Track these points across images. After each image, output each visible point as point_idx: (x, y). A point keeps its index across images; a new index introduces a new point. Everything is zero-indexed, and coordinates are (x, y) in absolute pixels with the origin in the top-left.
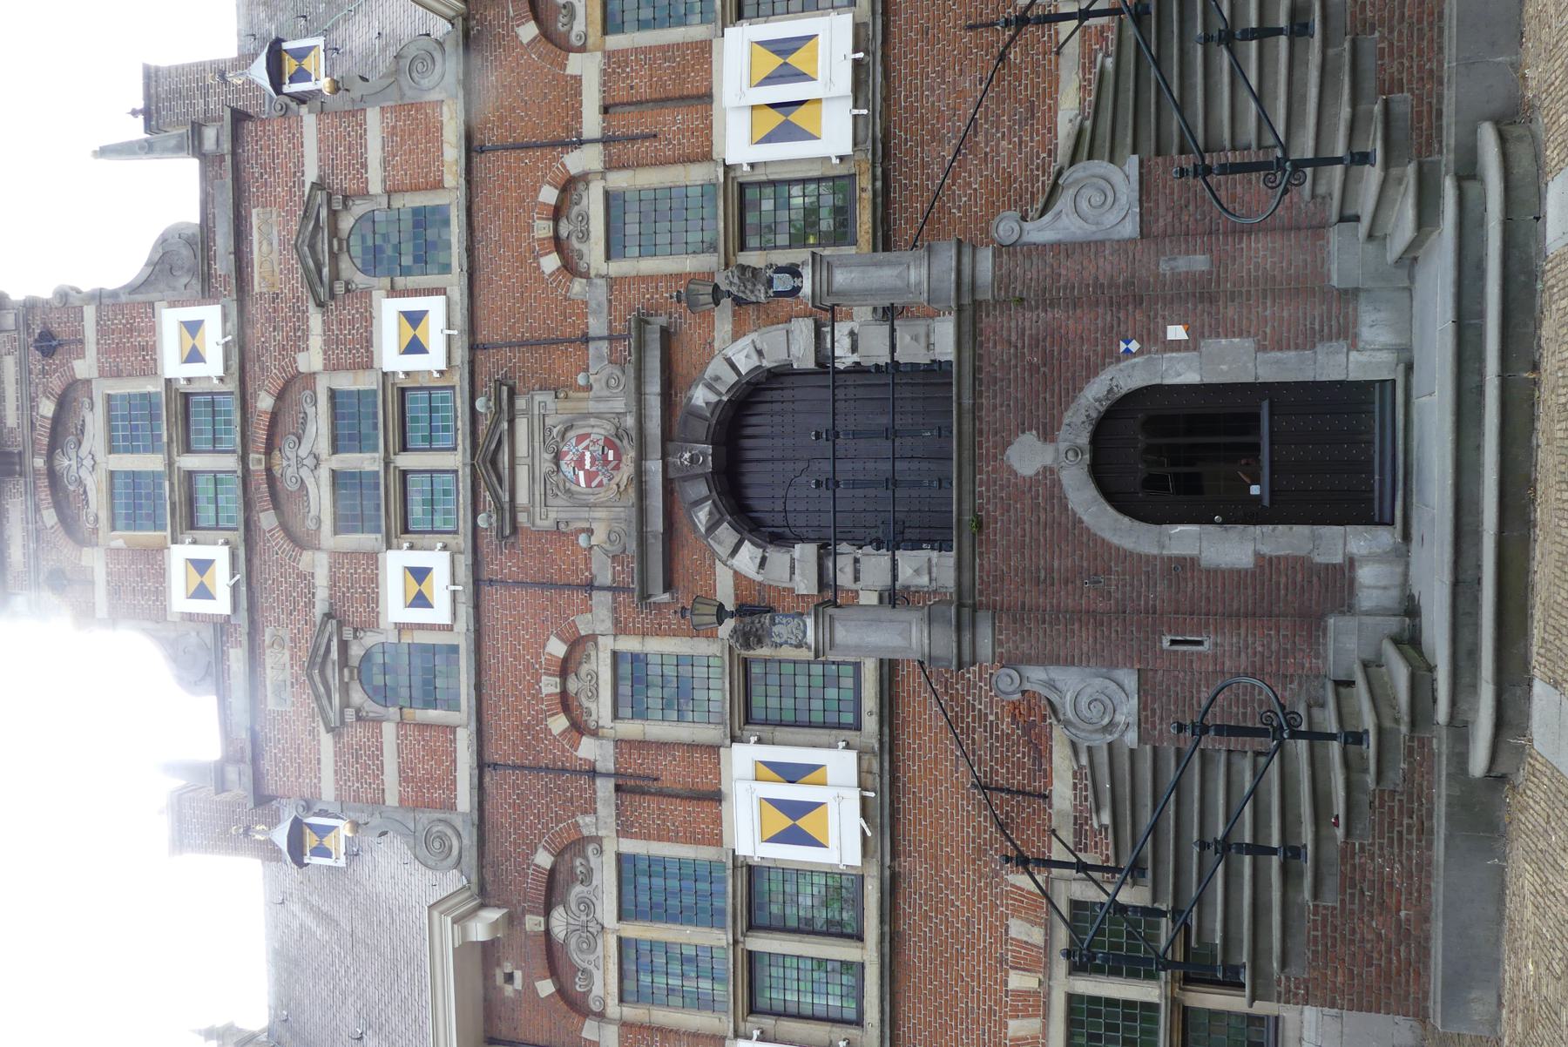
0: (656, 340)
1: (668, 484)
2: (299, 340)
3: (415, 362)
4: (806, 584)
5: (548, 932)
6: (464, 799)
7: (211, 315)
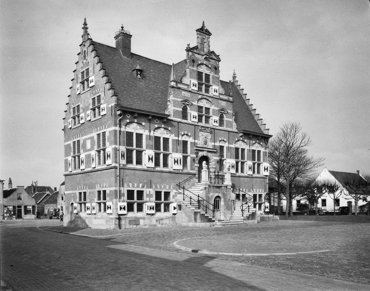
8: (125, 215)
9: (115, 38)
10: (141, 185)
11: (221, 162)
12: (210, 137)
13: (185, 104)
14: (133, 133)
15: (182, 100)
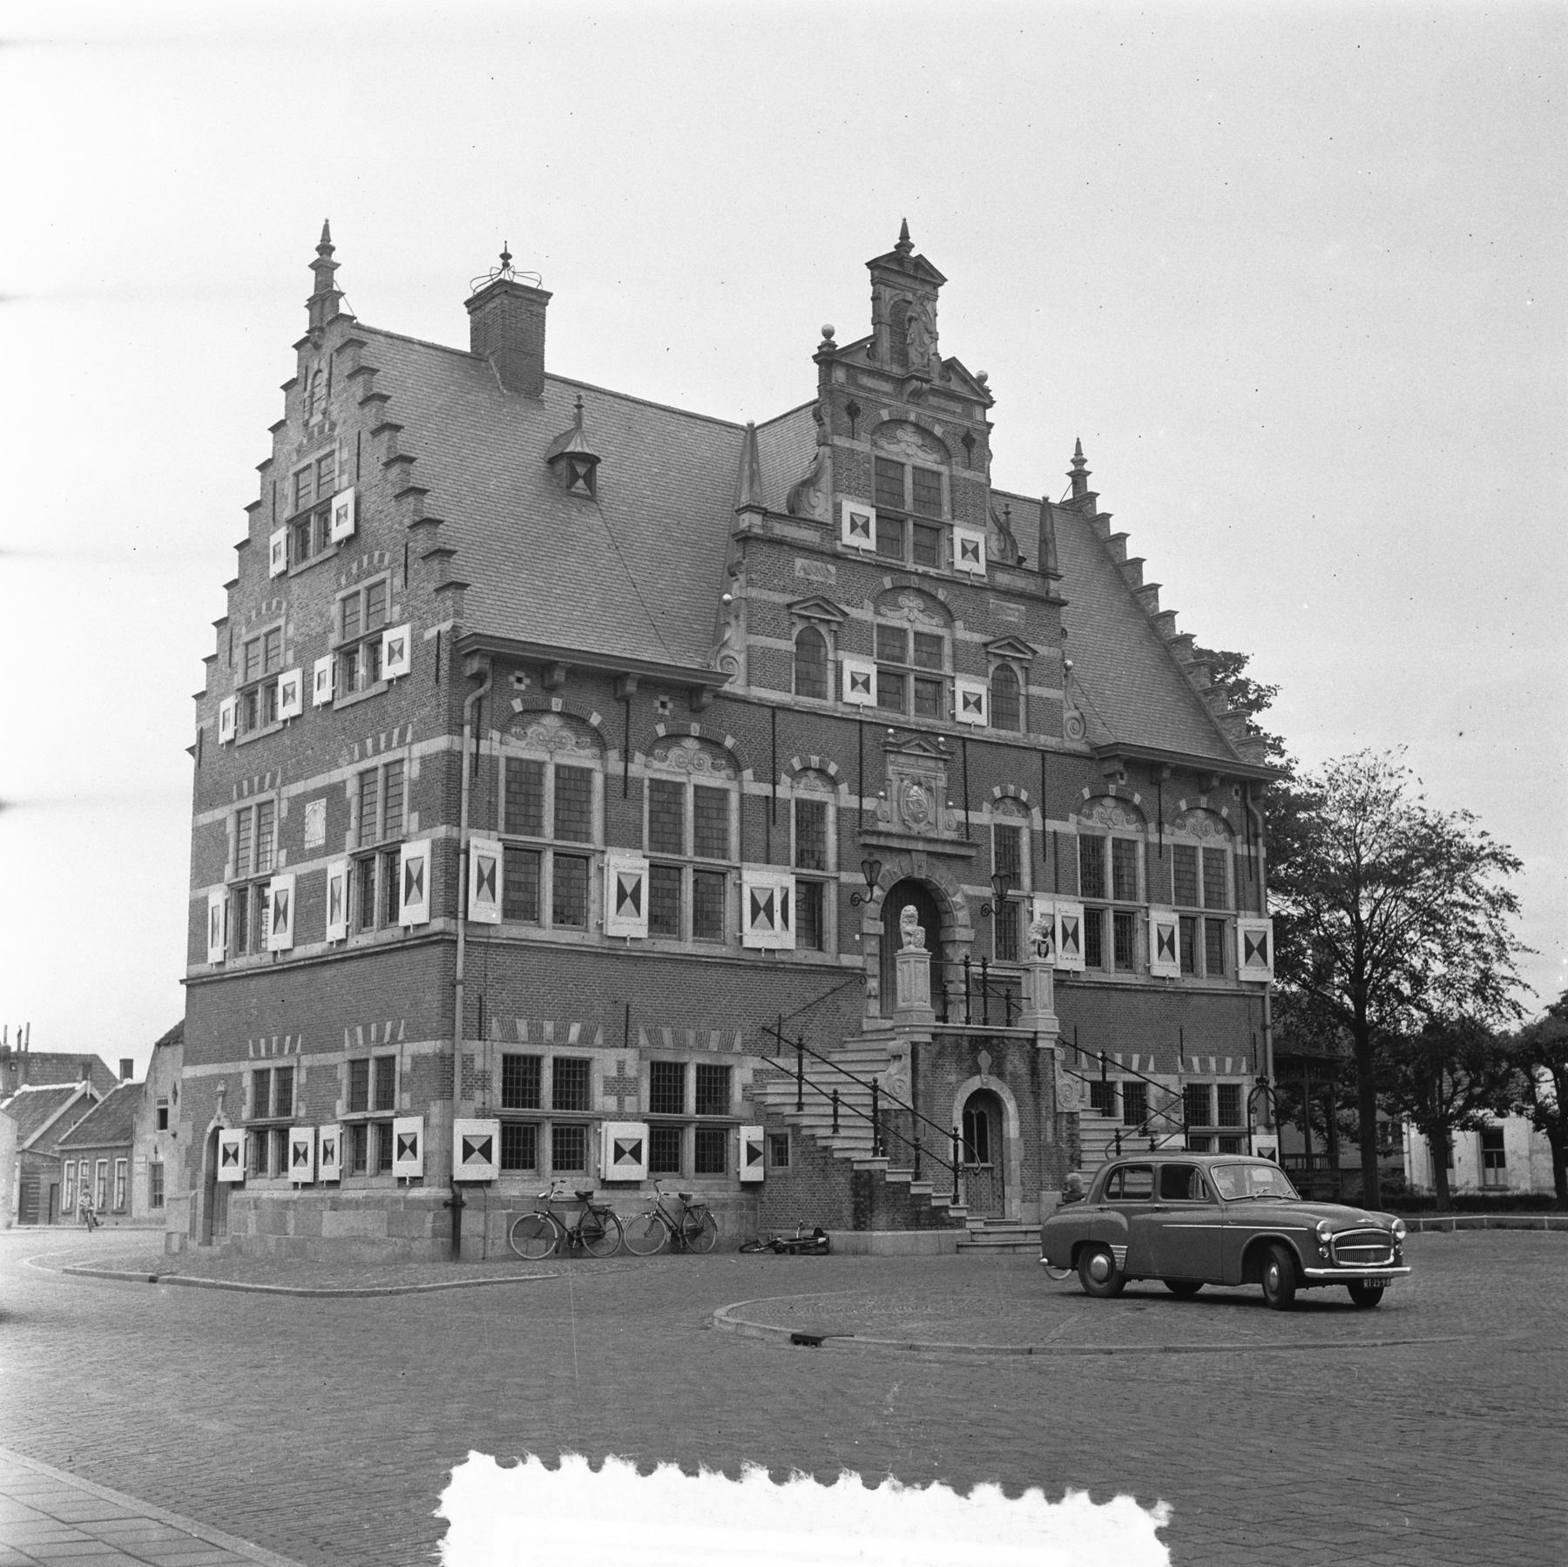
1: (909, 851)
5: (689, 736)
6: (758, 692)
8: (488, 1183)
9: (467, 303)
10: (575, 1030)
11: (1004, 917)
12: (942, 783)
13: (808, 618)
14: (541, 765)
15: (797, 598)
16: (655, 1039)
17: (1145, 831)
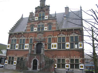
0: (44, 41)
1: (38, 41)
2: (46, 23)
3: (44, 29)
4: (35, 47)
6: (27, 32)
7: (47, 18)
16: (18, 56)
17: (66, 36)
